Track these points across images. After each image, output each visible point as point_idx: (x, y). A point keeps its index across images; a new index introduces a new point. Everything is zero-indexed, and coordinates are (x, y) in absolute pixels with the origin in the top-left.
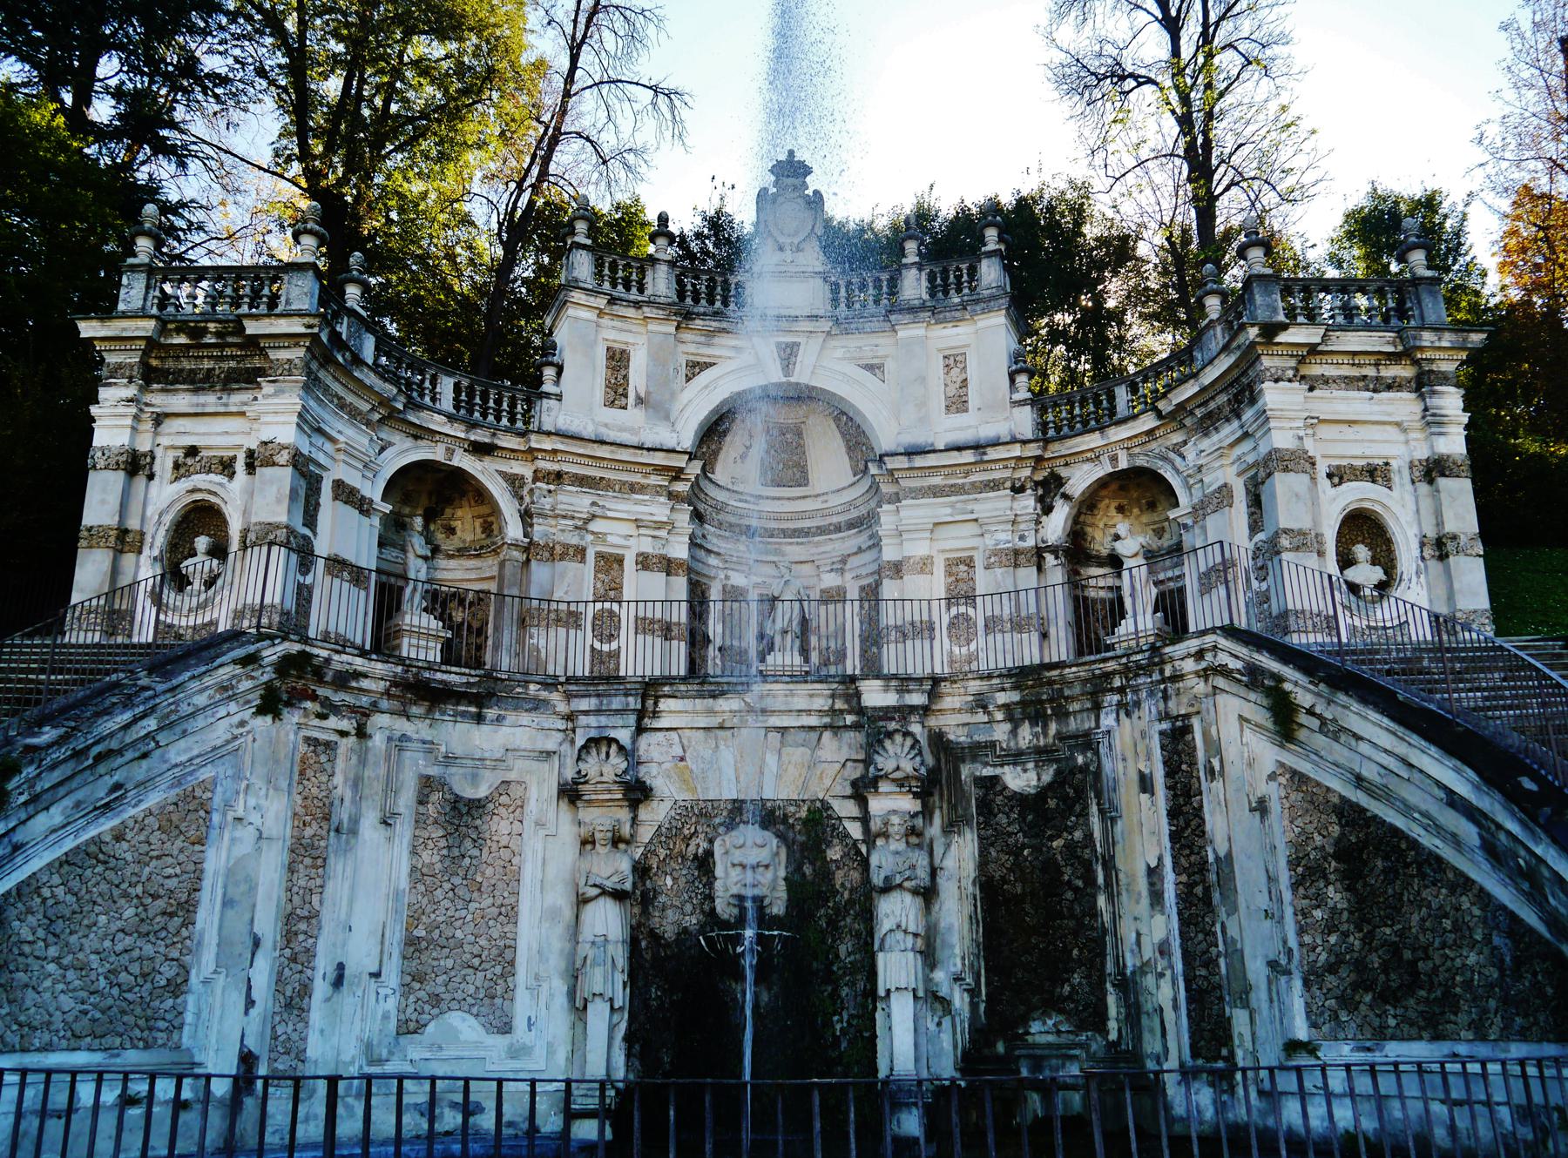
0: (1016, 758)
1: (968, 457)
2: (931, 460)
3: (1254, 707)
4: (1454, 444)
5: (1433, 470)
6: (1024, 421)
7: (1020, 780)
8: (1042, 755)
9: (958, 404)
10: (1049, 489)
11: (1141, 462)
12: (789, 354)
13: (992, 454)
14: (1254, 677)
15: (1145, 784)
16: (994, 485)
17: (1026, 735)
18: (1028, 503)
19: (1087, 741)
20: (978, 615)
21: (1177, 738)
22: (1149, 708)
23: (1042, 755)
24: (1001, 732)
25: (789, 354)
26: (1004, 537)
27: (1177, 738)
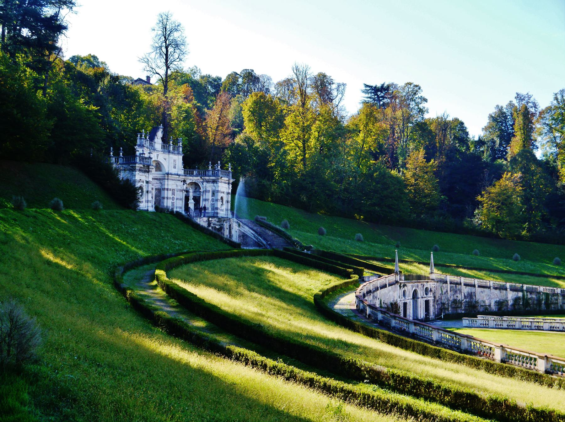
0: (217, 225)
1: (178, 176)
2: (172, 176)
3: (237, 224)
4: (230, 191)
5: (228, 193)
6: (182, 172)
7: (217, 227)
8: (219, 225)
9: (175, 167)
10: (184, 181)
11: (196, 182)
12: (158, 155)
13: (181, 177)
14: (237, 222)
15: (227, 229)
16: (179, 180)
17: (218, 223)
18: (182, 183)
19: (223, 225)
20: (175, 197)
21: (230, 226)
22: (228, 223)
23: (219, 225)
24: (216, 223)
25: (158, 155)
26: (179, 188)
27: (230, 226)
